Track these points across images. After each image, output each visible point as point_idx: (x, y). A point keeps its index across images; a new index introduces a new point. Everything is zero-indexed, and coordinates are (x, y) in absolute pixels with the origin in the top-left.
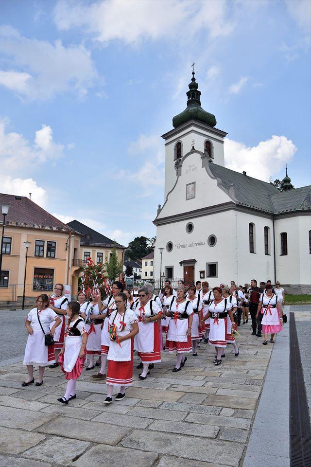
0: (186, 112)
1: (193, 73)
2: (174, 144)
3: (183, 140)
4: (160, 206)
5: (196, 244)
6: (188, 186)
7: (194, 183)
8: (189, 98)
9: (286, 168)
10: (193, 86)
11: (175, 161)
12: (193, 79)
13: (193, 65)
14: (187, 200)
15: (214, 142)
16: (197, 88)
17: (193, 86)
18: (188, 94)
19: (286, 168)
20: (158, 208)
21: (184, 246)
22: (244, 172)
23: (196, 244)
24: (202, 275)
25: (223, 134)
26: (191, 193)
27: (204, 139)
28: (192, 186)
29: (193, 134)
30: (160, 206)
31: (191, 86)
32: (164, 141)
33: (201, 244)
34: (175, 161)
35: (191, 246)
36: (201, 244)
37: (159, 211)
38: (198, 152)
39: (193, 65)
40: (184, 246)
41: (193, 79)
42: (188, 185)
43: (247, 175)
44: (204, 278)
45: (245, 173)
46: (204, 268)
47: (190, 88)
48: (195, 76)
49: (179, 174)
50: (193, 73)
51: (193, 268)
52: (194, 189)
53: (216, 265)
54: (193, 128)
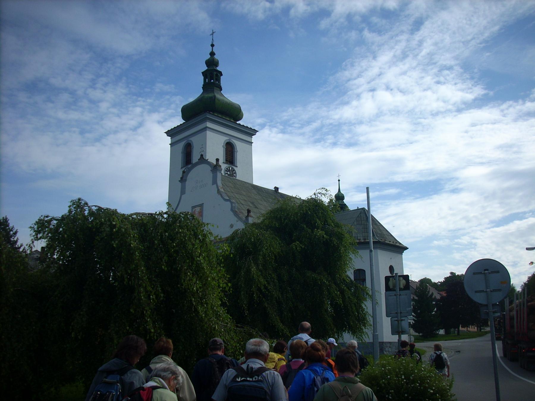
0: (199, 100)
1: (213, 45)
3: (194, 140)
6: (194, 210)
7: (201, 206)
8: (205, 80)
9: (339, 180)
10: (212, 63)
11: (183, 169)
12: (212, 54)
13: (212, 34)
15: (239, 146)
16: (217, 66)
17: (212, 63)
18: (204, 74)
19: (339, 180)
22: (275, 188)
25: (251, 132)
27: (223, 139)
38: (209, 163)
39: (212, 34)
41: (212, 54)
43: (279, 191)
45: (277, 189)
47: (207, 66)
49: (183, 192)
50: (213, 45)
54: (209, 124)
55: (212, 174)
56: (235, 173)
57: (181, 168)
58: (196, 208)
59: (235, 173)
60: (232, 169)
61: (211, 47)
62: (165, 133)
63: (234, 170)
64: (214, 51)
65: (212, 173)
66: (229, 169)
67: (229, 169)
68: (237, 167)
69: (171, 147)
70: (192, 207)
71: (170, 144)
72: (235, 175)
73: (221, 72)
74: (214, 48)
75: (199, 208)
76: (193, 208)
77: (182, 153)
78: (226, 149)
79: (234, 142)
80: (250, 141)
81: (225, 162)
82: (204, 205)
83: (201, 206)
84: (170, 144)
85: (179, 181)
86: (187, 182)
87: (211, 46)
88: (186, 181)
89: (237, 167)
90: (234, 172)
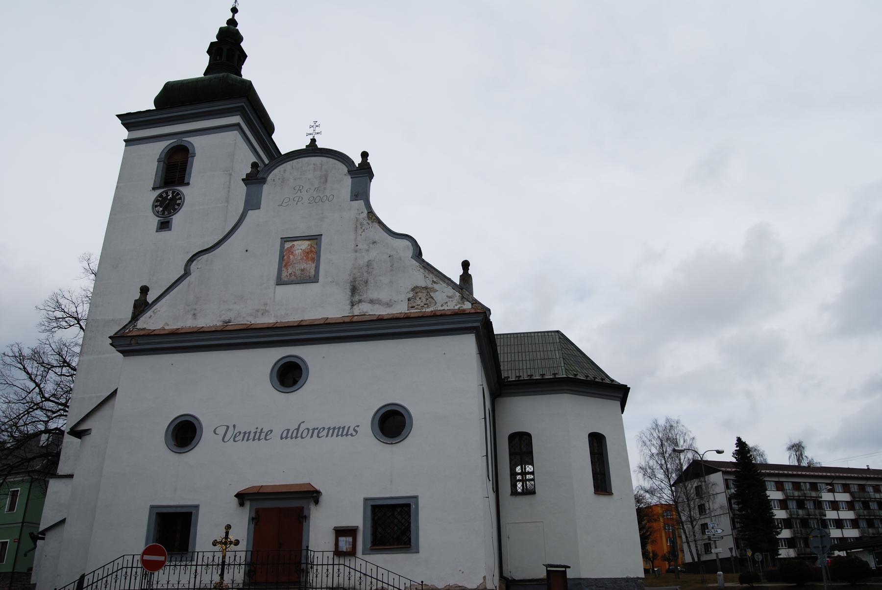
1: (234, 10)
2: (159, 147)
3: (197, 142)
4: (144, 290)
5: (316, 432)
6: (287, 245)
7: (316, 239)
11: (159, 192)
12: (232, 22)
14: (280, 282)
20: (137, 296)
21: (261, 435)
23: (316, 432)
24: (345, 543)
26: (303, 266)
28: (304, 245)
29: (235, 135)
30: (144, 290)
31: (222, 33)
32: (124, 133)
33: (341, 431)
34: (159, 192)
35: (286, 435)
36: (341, 431)
37: (141, 307)
40: (261, 435)
41: (232, 22)
42: (285, 240)
44: (352, 553)
46: (356, 518)
48: (237, 17)
49: (252, 203)
50: (234, 10)
51: (300, 518)
52: (314, 255)
55: (350, 180)
57: (154, 189)
58: (296, 243)
61: (232, 14)
62: (118, 116)
65: (352, 178)
69: (126, 146)
70: (281, 238)
71: (125, 141)
73: (247, 56)
75: (308, 243)
76: (285, 240)
77: (159, 161)
82: (323, 238)
83: (316, 239)
84: (125, 141)
85: (243, 180)
86: (266, 188)
87: (232, 12)
88: (264, 184)
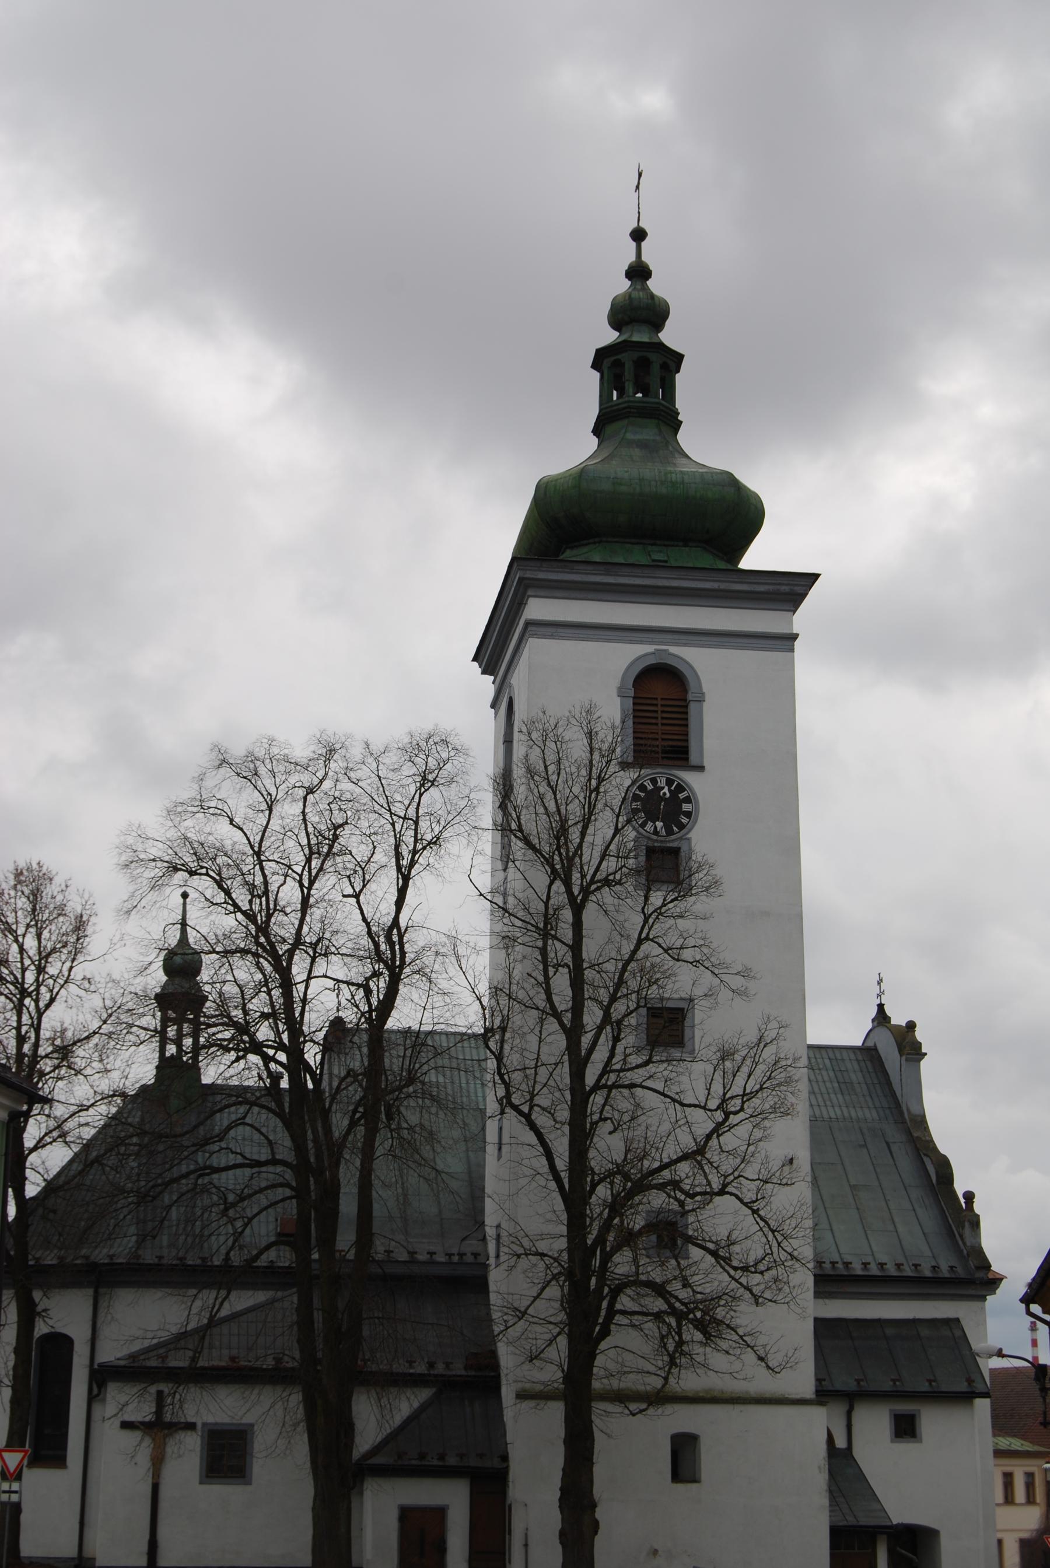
1: (639, 235)
12: (639, 272)
41: (639, 272)
50: (639, 235)
53: (244, 1477)
56: (688, 800)
59: (688, 800)
60: (669, 782)
61: (634, 244)
63: (680, 788)
64: (644, 258)
66: (650, 787)
67: (650, 787)
68: (701, 768)
72: (686, 807)
74: (643, 244)
78: (634, 698)
79: (682, 655)
80: (788, 631)
81: (630, 759)
87: (634, 239)
89: (701, 768)
90: (682, 796)
